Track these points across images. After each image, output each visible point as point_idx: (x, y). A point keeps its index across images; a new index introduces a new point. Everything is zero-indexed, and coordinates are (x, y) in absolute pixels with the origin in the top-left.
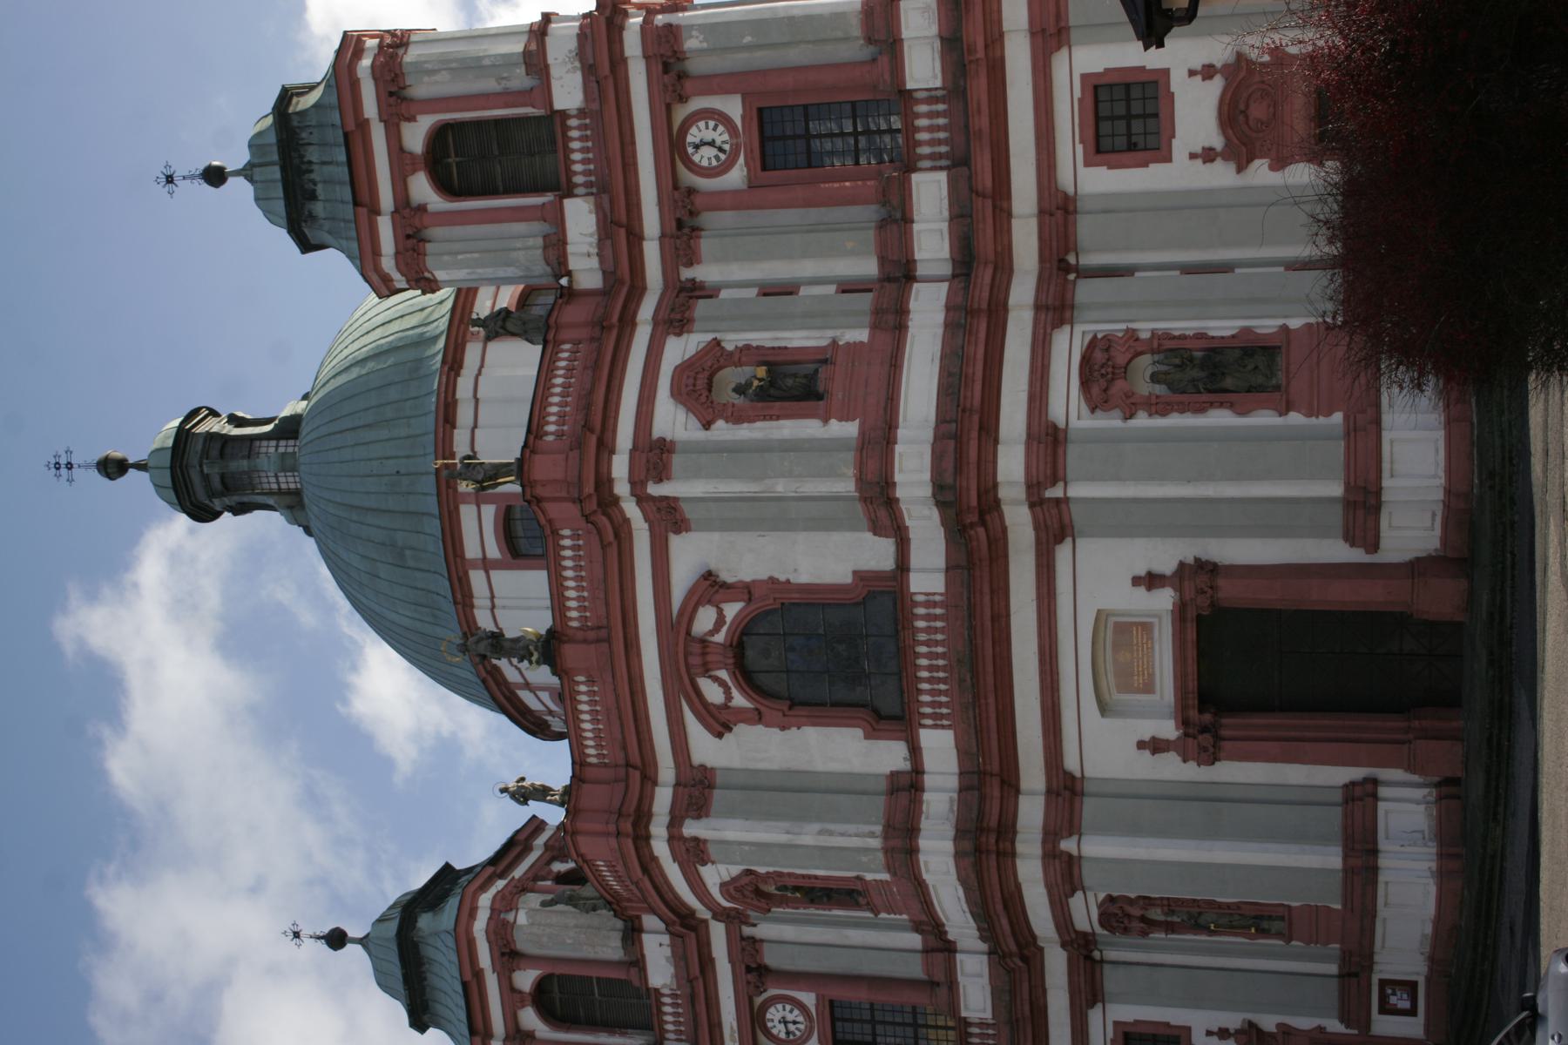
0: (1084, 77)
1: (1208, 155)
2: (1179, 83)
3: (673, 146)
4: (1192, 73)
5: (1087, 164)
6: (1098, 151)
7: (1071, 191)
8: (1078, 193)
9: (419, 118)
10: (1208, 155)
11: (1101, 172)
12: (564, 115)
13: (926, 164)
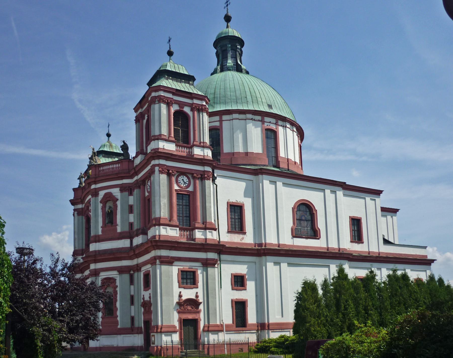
1: (180, 296)
2: (195, 290)
3: (182, 172)
4: (197, 293)
5: (178, 269)
6: (182, 271)
9: (191, 112)
10: (180, 296)
12: (191, 147)
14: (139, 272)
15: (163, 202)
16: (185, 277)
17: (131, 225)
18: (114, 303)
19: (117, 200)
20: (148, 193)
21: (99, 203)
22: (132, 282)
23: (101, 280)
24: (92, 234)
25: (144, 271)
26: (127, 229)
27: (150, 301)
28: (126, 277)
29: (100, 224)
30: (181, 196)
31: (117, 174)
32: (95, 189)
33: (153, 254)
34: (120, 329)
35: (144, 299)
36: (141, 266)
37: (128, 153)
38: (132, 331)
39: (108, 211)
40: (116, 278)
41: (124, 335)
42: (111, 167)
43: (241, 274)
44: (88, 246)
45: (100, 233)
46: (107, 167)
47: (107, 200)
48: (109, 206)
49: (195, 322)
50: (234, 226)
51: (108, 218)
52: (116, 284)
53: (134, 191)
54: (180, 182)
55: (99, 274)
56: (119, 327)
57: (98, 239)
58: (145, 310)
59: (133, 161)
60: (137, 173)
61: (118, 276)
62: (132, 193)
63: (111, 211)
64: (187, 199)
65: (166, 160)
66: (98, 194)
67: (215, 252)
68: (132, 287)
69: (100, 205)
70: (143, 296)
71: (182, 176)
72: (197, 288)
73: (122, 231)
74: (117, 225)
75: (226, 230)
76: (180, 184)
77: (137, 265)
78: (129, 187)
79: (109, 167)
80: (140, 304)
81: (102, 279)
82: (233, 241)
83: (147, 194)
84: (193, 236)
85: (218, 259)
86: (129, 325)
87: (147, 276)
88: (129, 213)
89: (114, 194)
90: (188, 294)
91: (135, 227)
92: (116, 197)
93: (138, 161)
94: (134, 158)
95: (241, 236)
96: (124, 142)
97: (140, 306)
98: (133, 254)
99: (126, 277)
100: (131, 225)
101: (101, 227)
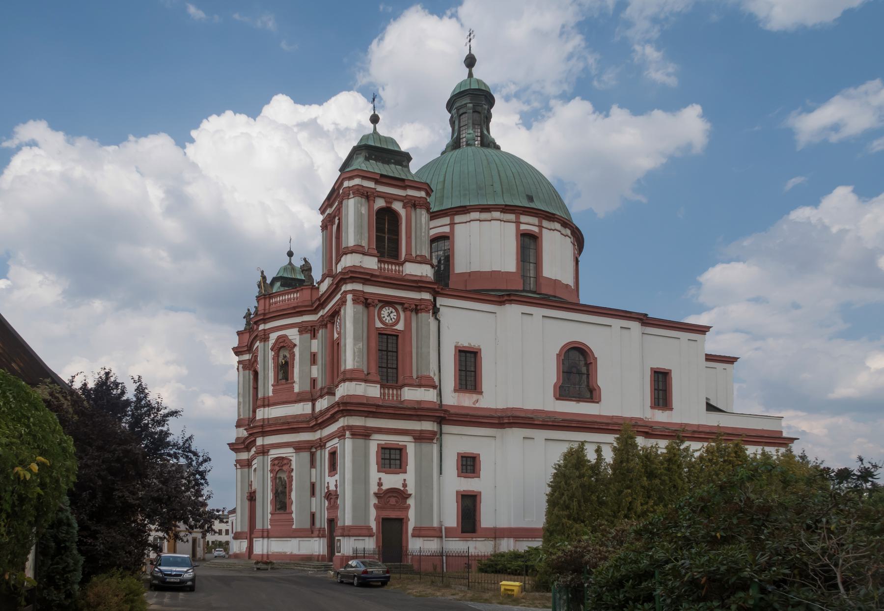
0: (406, 446)
1: (380, 484)
2: (401, 477)
4: (405, 480)
6: (382, 448)
7: (371, 438)
8: (371, 441)
10: (380, 484)
11: (376, 449)
13: (382, 392)
14: (323, 450)
15: (358, 347)
16: (387, 456)
17: (314, 381)
18: (288, 494)
19: (295, 345)
20: (338, 334)
21: (270, 351)
22: (313, 464)
23: (271, 461)
24: (260, 395)
25: (329, 448)
26: (307, 388)
27: (336, 491)
28: (306, 455)
29: (271, 381)
30: (385, 337)
31: (294, 308)
32: (264, 330)
33: (342, 422)
34: (296, 530)
35: (328, 487)
36: (325, 441)
37: (311, 276)
39: (282, 362)
40: (291, 458)
42: (287, 297)
43: (473, 453)
44: (254, 412)
45: (271, 394)
46: (281, 298)
47: (280, 346)
48: (283, 355)
49: (401, 522)
50: (463, 382)
51: (282, 371)
52: (292, 467)
53: (318, 332)
54: (384, 317)
55: (268, 452)
56: (294, 527)
57: (267, 403)
58: (330, 503)
59: (318, 288)
60: (322, 305)
61: (294, 454)
62: (316, 334)
63: (286, 363)
64: (395, 342)
65: (364, 284)
66: (269, 338)
67: (434, 421)
68: (313, 470)
69: (271, 354)
70: (328, 483)
71: (387, 308)
72: (405, 472)
73: (301, 390)
74: (294, 382)
75: (453, 388)
76: (384, 319)
77: (320, 439)
78: (311, 326)
79: (284, 298)
80: (323, 495)
82: (461, 405)
83: (336, 336)
84: (400, 397)
85: (439, 432)
86: (308, 525)
87: (333, 454)
88: (311, 365)
89: (290, 338)
90: (392, 481)
91: (319, 385)
92: (293, 341)
93: (324, 287)
94: (319, 283)
95: (475, 397)
96: (305, 259)
97: (323, 498)
98: (314, 423)
99: (306, 455)
100: (314, 381)
101: (272, 385)
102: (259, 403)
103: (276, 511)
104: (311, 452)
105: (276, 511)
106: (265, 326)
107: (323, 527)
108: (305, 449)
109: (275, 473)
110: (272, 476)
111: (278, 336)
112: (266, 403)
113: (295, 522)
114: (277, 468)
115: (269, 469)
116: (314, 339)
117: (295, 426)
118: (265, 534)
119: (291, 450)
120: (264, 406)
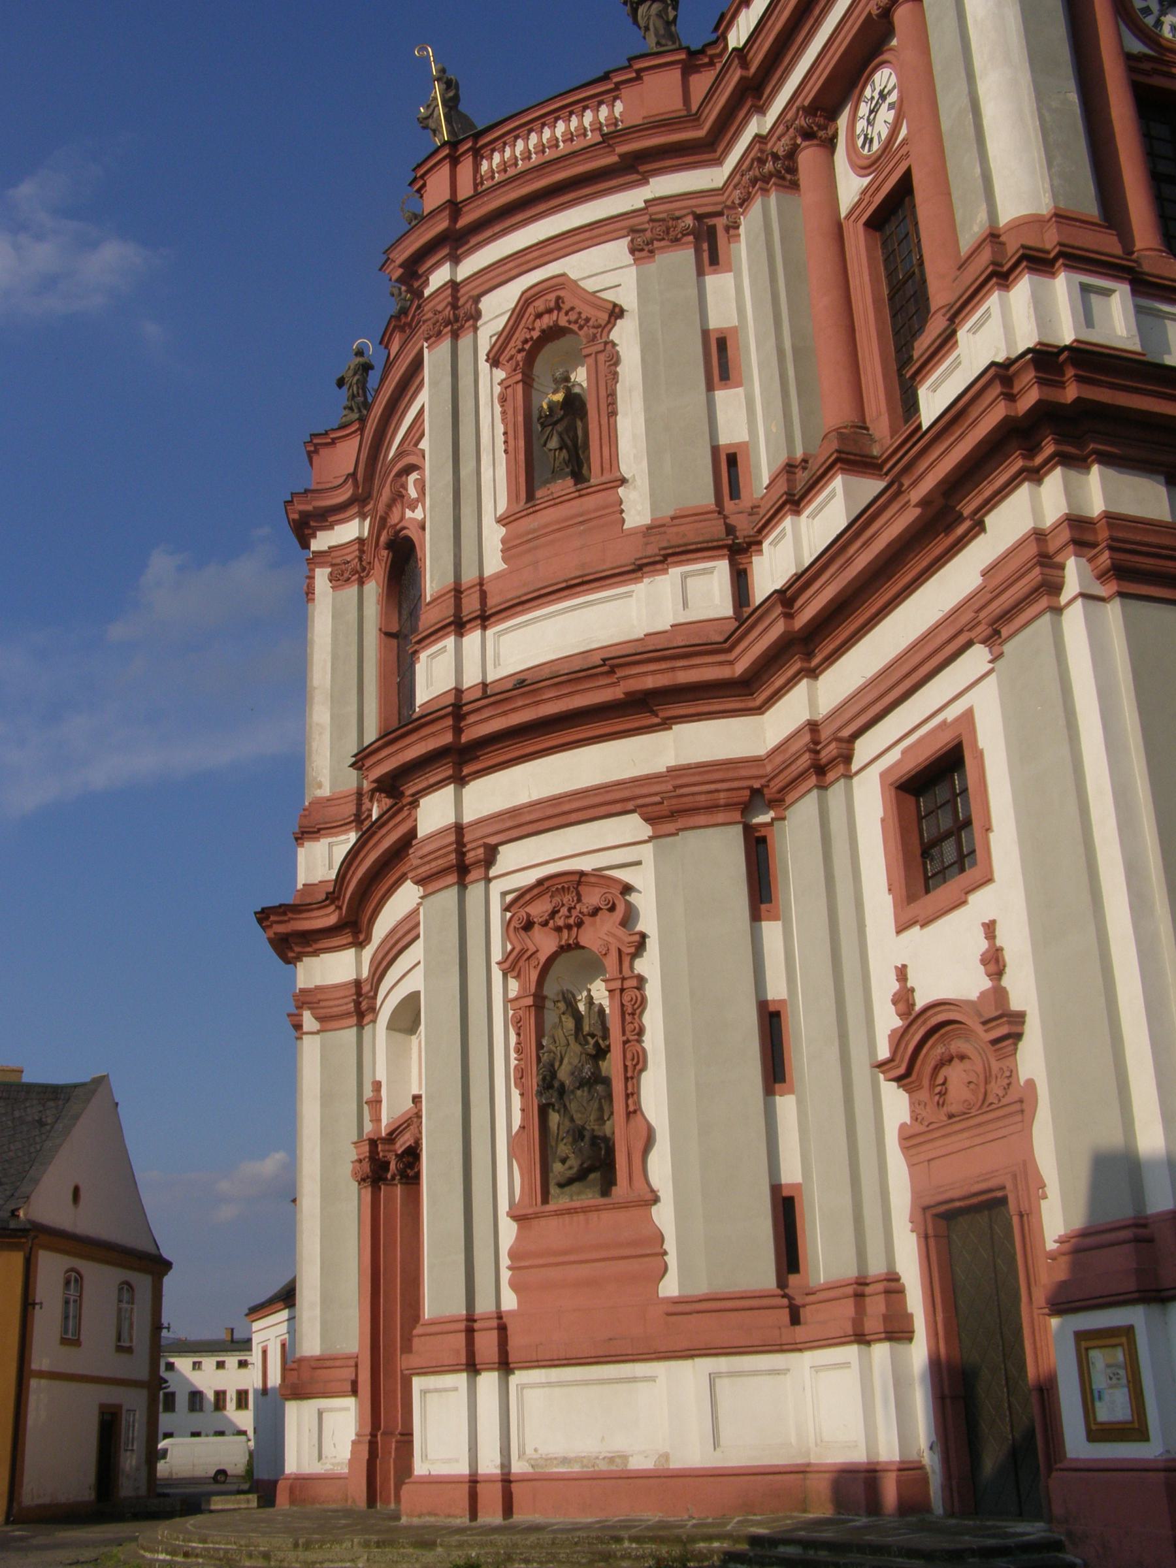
14: (840, 786)
19: (617, 312)
21: (484, 366)
23: (507, 909)
34: (682, 1307)
38: (795, 1320)
41: (722, 1363)
45: (494, 564)
47: (536, 334)
56: (670, 1287)
61: (646, 853)
66: (477, 315)
78: (699, 218)
81: (509, 898)
89: (590, 285)
92: (609, 296)
102: (429, 618)
103: (545, 1199)
104: (748, 829)
105: (545, 1199)
106: (453, 272)
107: (876, 1268)
108: (712, 808)
109: (534, 975)
110: (512, 994)
111: (523, 293)
112: (471, 605)
113: (672, 1260)
114: (545, 943)
115: (497, 955)
116: (715, 272)
117: (650, 683)
118: (487, 1344)
119: (633, 826)
120: (459, 626)
